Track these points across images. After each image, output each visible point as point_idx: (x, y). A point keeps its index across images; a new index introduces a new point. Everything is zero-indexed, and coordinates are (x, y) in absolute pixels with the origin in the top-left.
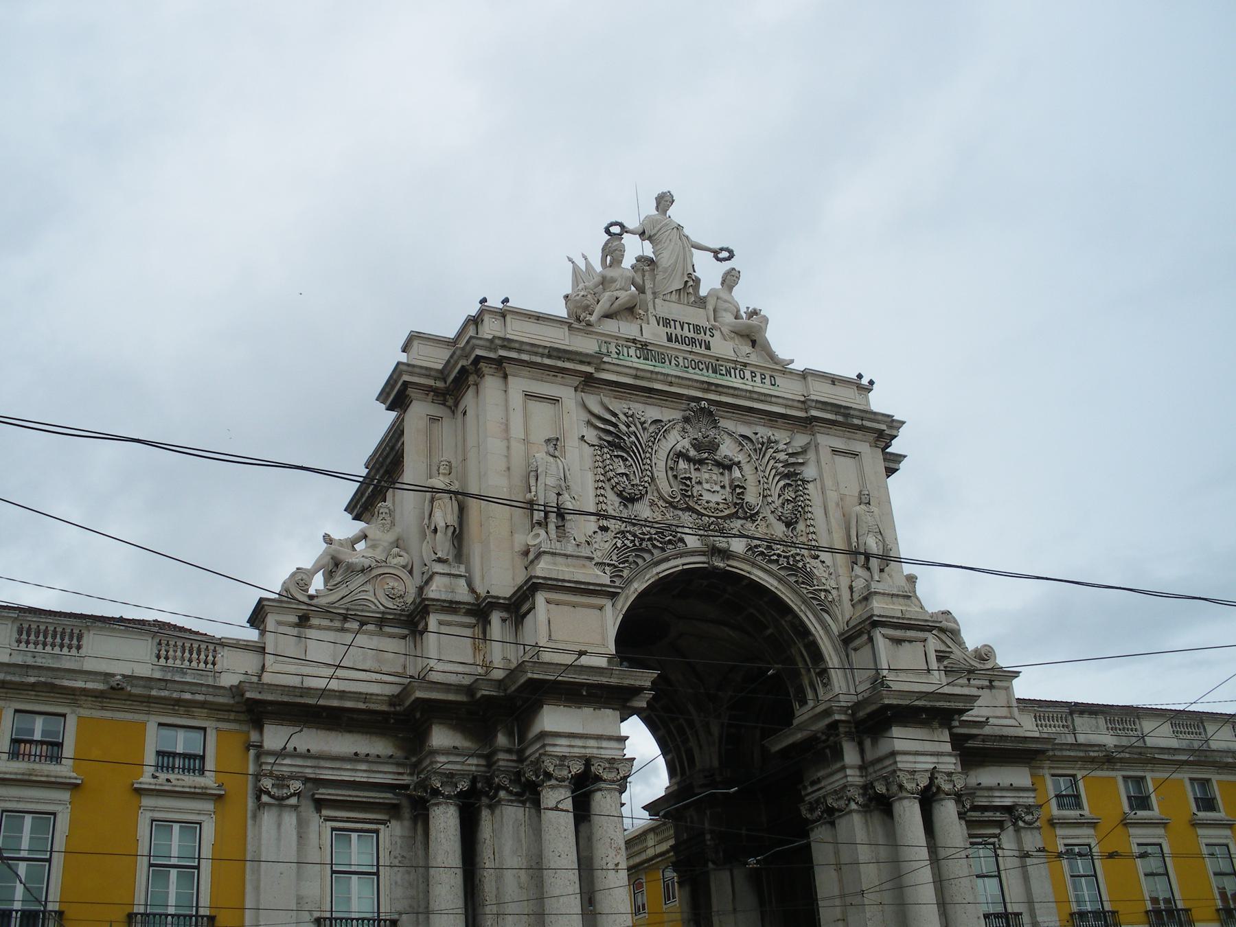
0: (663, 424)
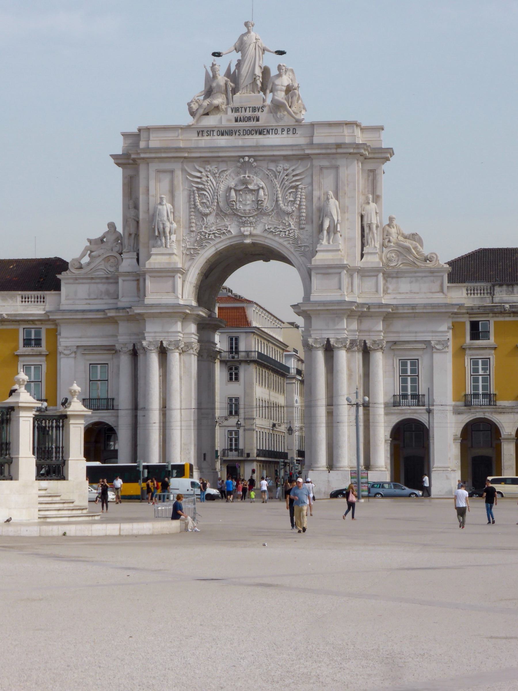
0: (226, 172)
